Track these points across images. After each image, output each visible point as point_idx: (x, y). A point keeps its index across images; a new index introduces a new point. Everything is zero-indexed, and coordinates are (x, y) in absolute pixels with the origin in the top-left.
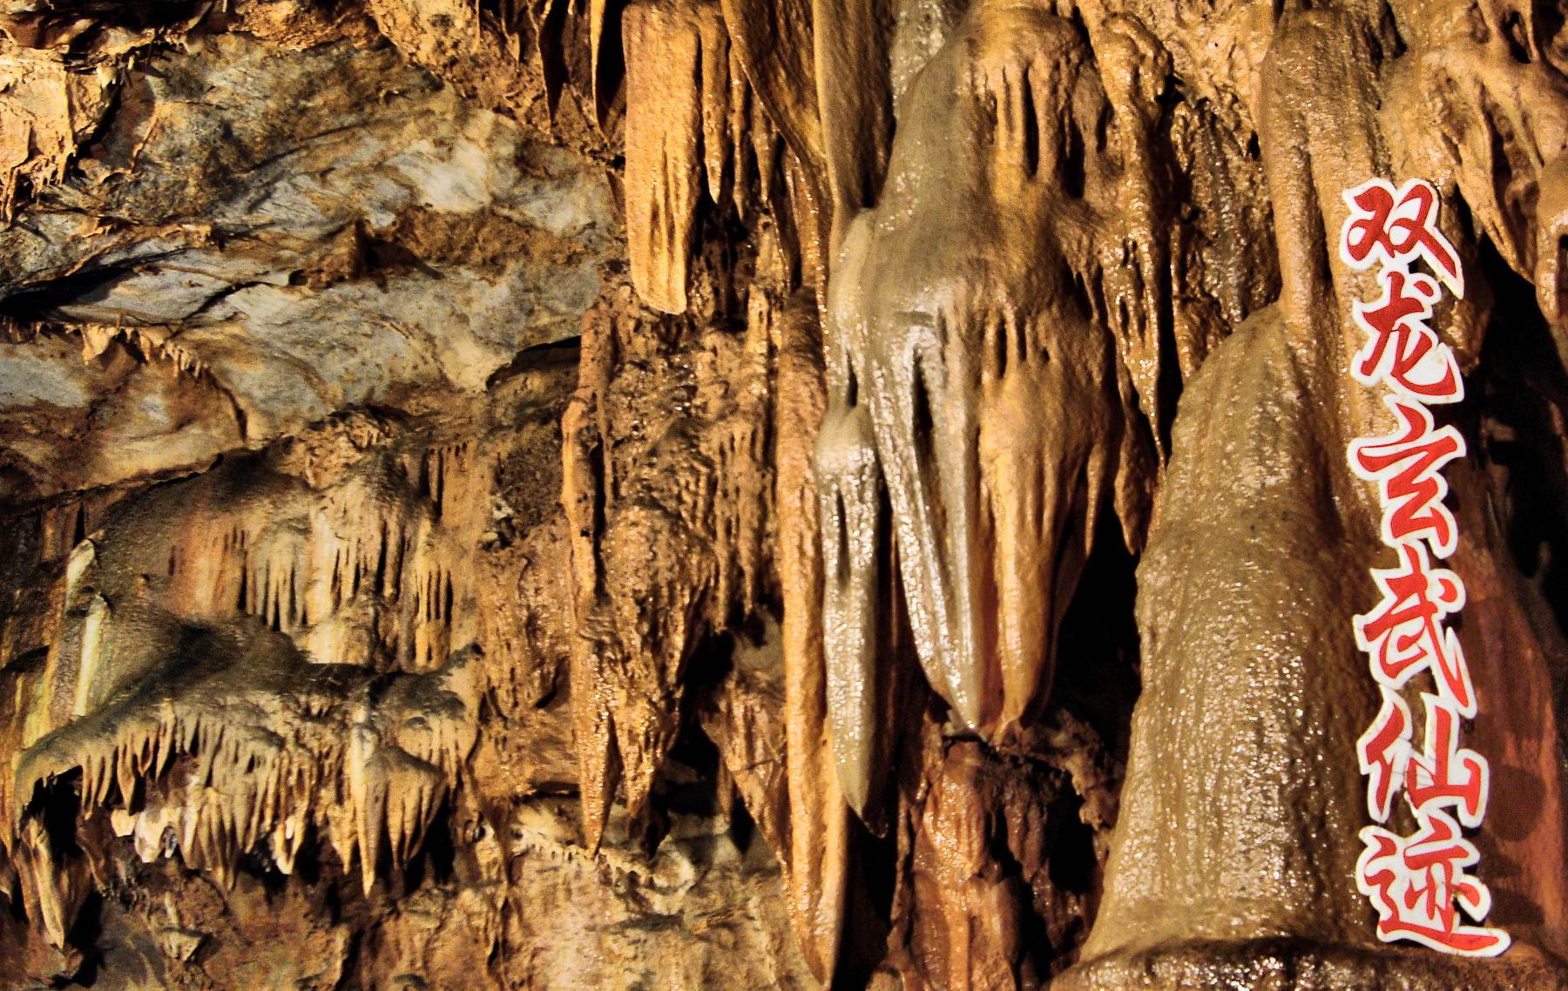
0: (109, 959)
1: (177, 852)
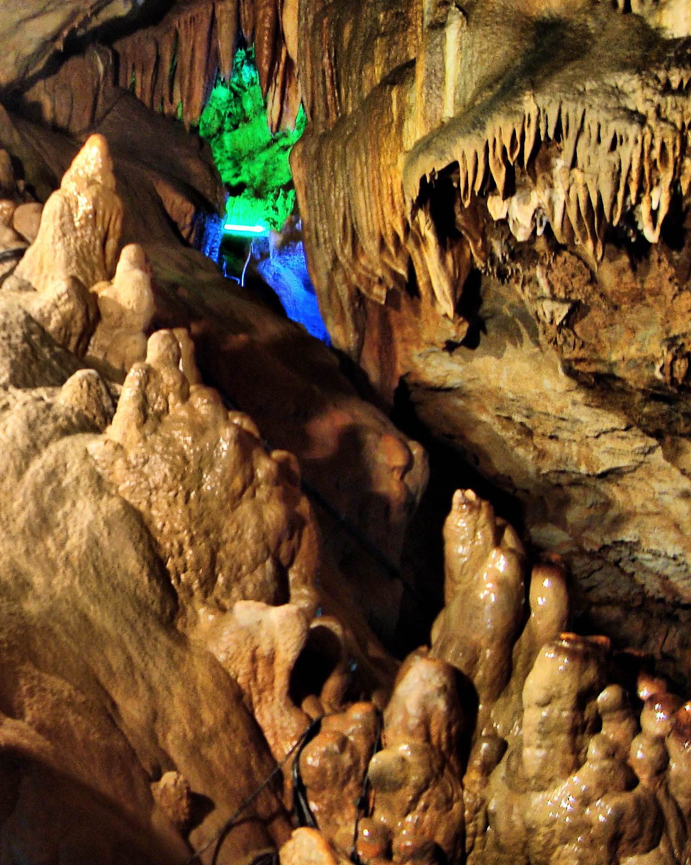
0: (490, 325)
1: (548, 231)
